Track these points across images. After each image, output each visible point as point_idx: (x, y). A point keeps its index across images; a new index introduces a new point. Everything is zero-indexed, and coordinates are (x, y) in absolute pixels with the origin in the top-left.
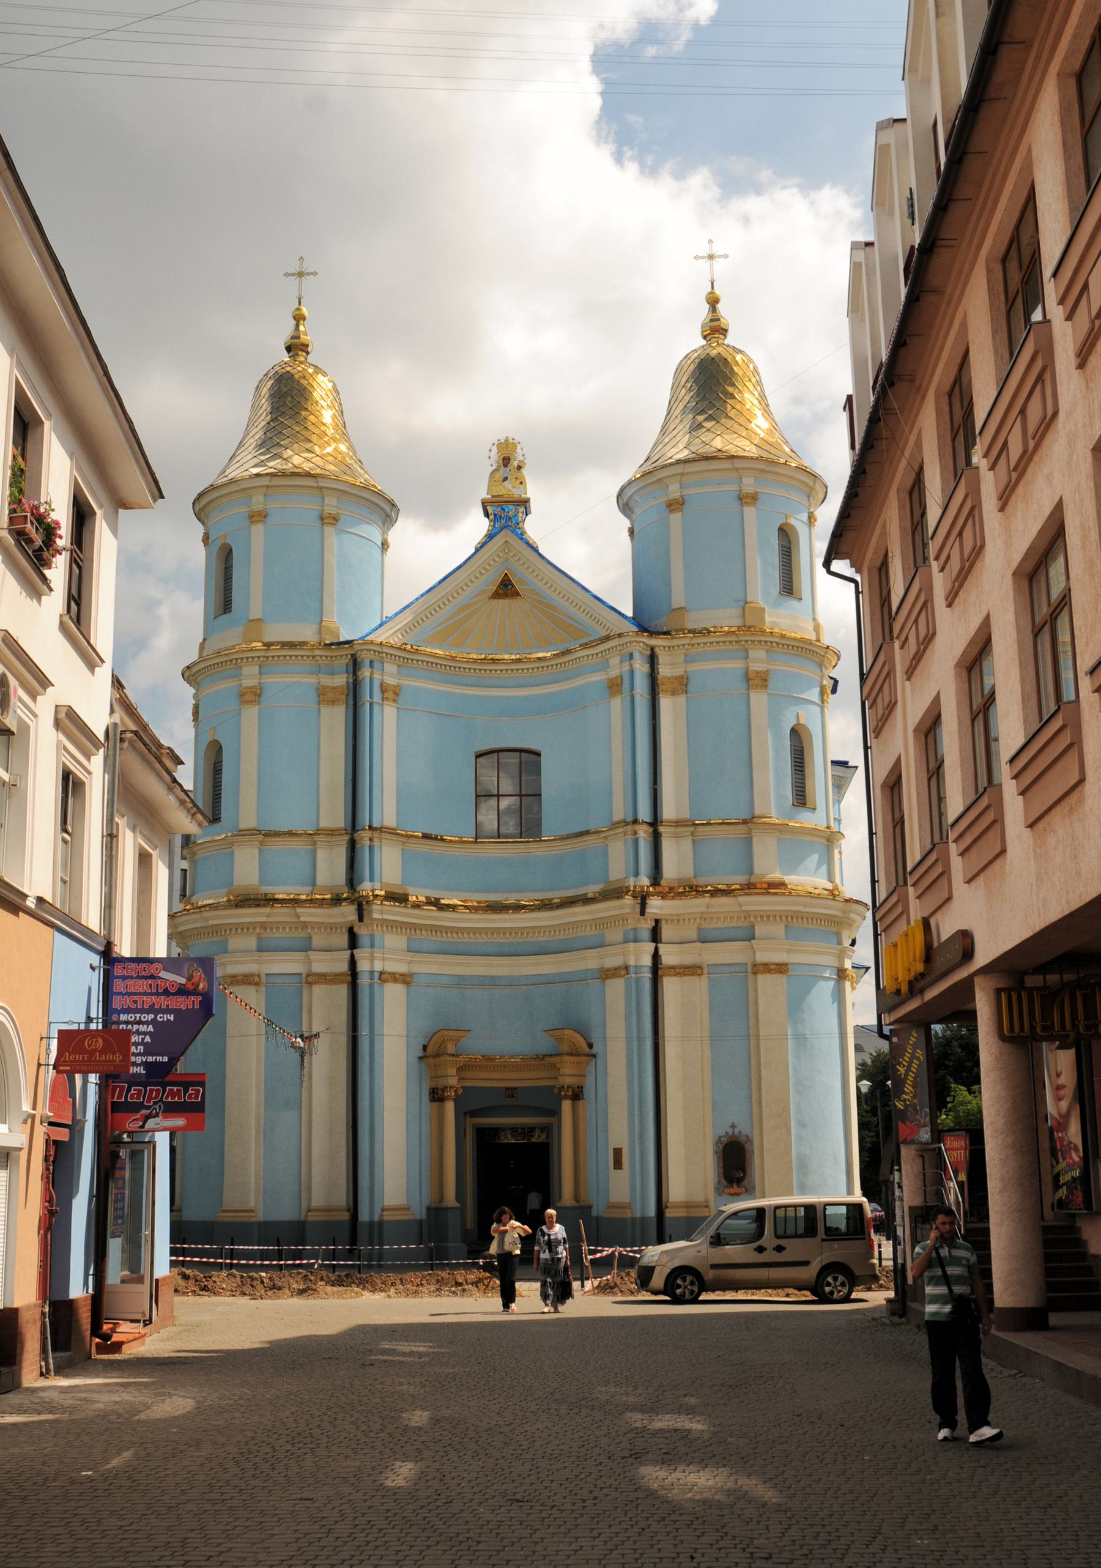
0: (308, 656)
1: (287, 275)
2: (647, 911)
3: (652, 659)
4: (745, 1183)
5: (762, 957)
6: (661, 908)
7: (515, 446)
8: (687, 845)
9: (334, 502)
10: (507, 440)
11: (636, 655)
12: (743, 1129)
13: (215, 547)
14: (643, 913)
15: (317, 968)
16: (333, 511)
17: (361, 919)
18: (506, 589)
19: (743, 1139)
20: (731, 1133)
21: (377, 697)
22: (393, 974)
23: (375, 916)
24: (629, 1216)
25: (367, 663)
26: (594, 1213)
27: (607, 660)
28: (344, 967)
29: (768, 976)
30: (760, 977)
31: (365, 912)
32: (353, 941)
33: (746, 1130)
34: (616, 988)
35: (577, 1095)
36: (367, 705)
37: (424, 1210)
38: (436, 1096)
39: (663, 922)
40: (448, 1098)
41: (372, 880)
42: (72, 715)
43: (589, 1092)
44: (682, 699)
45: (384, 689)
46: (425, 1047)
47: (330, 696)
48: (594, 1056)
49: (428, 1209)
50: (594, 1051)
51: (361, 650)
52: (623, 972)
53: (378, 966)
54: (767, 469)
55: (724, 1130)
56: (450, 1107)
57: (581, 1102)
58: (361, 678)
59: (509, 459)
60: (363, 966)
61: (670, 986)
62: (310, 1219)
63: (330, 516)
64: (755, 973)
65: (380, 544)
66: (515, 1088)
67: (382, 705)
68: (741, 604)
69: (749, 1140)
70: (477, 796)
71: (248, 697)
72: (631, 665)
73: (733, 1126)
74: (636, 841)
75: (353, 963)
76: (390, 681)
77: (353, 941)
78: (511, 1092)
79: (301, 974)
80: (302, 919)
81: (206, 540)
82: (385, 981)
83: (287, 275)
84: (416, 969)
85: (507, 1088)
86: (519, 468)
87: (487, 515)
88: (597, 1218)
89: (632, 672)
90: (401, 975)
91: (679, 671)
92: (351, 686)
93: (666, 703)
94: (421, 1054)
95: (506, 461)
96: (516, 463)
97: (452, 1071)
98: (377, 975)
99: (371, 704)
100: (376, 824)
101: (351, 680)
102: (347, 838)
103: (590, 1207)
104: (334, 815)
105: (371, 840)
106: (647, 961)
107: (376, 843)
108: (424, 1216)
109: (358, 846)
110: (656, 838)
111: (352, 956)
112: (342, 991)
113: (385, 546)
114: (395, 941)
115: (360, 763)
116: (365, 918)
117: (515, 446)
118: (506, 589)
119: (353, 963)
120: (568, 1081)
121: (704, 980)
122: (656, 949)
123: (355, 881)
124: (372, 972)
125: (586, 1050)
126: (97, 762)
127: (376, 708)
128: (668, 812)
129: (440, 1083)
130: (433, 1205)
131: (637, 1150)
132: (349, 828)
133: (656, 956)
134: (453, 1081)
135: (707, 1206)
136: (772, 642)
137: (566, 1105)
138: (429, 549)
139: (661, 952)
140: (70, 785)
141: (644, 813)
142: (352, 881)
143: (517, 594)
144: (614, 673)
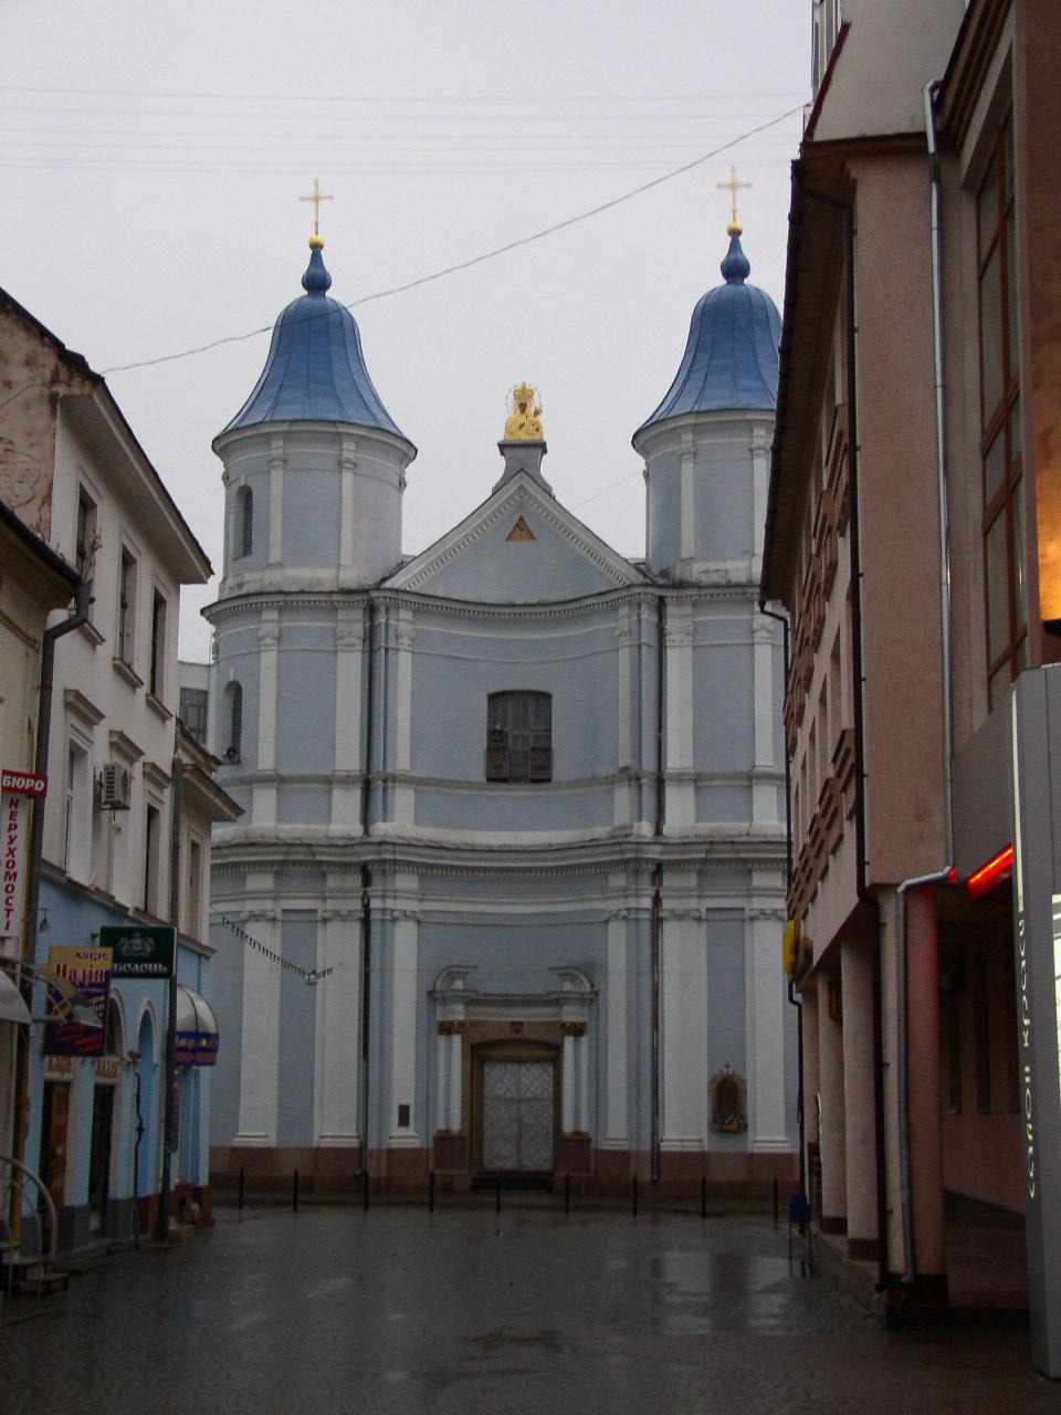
1: (302, 199)
6: (662, 853)
8: (690, 790)
9: (353, 447)
13: (235, 488)
15: (331, 905)
16: (350, 456)
19: (735, 1080)
22: (405, 911)
25: (383, 609)
26: (593, 1145)
27: (616, 609)
28: (357, 905)
32: (367, 881)
37: (431, 1141)
40: (456, 1032)
41: (385, 820)
42: (154, 766)
49: (435, 1139)
52: (625, 913)
53: (390, 904)
56: (457, 1040)
58: (376, 623)
60: (375, 904)
61: (670, 930)
63: (348, 461)
64: (752, 919)
65: (397, 483)
66: (521, 1023)
67: (398, 650)
69: (743, 1082)
71: (268, 641)
72: (639, 615)
73: (727, 1066)
74: (640, 787)
76: (404, 628)
77: (367, 881)
78: (517, 1026)
79: (315, 911)
80: (318, 858)
81: (226, 478)
82: (394, 920)
83: (302, 199)
84: (428, 906)
85: (513, 1023)
86: (537, 413)
87: (502, 454)
88: (597, 1151)
89: (639, 621)
90: (412, 912)
92: (368, 631)
94: (430, 988)
98: (388, 913)
99: (387, 649)
100: (389, 770)
102: (362, 780)
103: (589, 1140)
104: (349, 760)
105: (385, 781)
106: (647, 903)
107: (390, 784)
108: (431, 1144)
109: (372, 786)
110: (660, 784)
112: (354, 931)
113: (402, 484)
114: (406, 882)
115: (375, 705)
118: (521, 530)
122: (658, 893)
123: (369, 820)
124: (384, 910)
126: (167, 795)
127: (390, 651)
129: (450, 1018)
132: (364, 771)
133: (657, 900)
134: (461, 1017)
137: (569, 1041)
138: (441, 496)
139: (662, 894)
140: (152, 813)
141: (649, 765)
142: (366, 821)
143: (532, 537)
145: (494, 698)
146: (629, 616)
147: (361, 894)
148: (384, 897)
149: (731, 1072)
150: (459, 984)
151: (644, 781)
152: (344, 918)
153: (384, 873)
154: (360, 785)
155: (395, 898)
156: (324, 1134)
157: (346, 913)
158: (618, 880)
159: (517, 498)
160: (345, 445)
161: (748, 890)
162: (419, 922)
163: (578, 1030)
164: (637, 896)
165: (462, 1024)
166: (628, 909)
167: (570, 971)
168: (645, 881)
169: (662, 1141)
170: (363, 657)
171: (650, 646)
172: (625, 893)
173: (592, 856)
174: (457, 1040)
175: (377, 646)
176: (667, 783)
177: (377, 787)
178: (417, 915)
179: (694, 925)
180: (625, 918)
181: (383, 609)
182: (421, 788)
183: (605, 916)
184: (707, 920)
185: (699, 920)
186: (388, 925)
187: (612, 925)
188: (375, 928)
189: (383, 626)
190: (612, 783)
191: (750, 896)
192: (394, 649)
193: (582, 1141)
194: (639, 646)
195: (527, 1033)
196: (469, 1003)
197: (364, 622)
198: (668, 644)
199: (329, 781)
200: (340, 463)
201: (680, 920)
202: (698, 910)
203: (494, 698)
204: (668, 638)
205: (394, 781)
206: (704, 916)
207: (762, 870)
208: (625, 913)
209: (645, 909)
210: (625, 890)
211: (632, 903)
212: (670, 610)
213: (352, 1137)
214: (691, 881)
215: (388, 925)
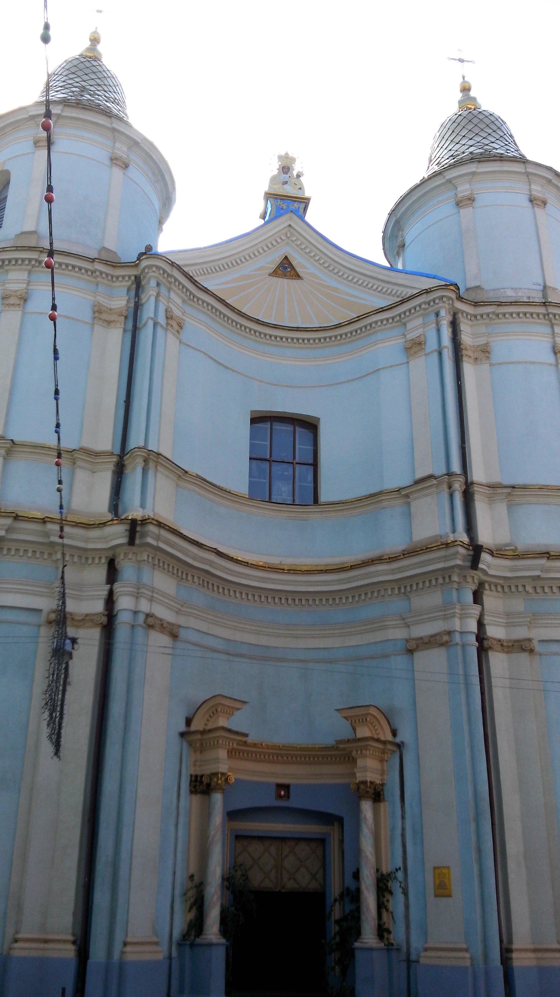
3: (454, 325)
7: (293, 160)
8: (501, 508)
9: (125, 149)
10: (287, 154)
11: (443, 313)
17: (131, 542)
18: (286, 269)
21: (162, 319)
23: (150, 540)
25: (153, 283)
27: (405, 324)
28: (99, 607)
31: (138, 535)
34: (432, 661)
35: (377, 795)
36: (151, 323)
38: (202, 786)
39: (487, 586)
40: (218, 788)
44: (485, 367)
45: (169, 317)
46: (188, 722)
47: (104, 316)
50: (398, 740)
51: (149, 267)
53: (144, 606)
57: (382, 805)
59: (289, 168)
60: (124, 603)
68: (541, 288)
70: (250, 459)
71: (12, 300)
74: (451, 496)
75: (110, 601)
79: (40, 611)
85: (280, 786)
86: (298, 176)
91: (482, 341)
95: (286, 169)
96: (295, 173)
97: (222, 754)
98: (141, 618)
100: (152, 446)
101: (132, 305)
102: (115, 459)
105: (146, 461)
107: (151, 465)
111: (111, 593)
114: (163, 582)
116: (137, 542)
117: (293, 160)
118: (286, 269)
119: (110, 601)
124: (136, 613)
125: (390, 737)
128: (478, 474)
129: (207, 770)
133: (481, 624)
134: (223, 768)
137: (367, 807)
143: (298, 276)
144: (410, 336)
145: (257, 419)
146: (424, 325)
147: (106, 593)
148: (137, 596)
154: (111, 467)
155: (151, 600)
156: (20, 936)
157: (81, 618)
158: (430, 599)
159: (283, 238)
160: (118, 145)
167: (372, 711)
170: (123, 337)
173: (393, 572)
175: (143, 322)
176: (477, 497)
177: (134, 469)
182: (181, 483)
183: (412, 645)
186: (140, 632)
188: (122, 634)
189: (153, 299)
192: (162, 326)
194: (440, 354)
195: (294, 802)
196: (232, 753)
197: (128, 302)
198: (464, 359)
200: (112, 160)
204: (464, 352)
205: (157, 463)
209: (471, 632)
212: (465, 328)
213: (65, 941)
215: (140, 632)
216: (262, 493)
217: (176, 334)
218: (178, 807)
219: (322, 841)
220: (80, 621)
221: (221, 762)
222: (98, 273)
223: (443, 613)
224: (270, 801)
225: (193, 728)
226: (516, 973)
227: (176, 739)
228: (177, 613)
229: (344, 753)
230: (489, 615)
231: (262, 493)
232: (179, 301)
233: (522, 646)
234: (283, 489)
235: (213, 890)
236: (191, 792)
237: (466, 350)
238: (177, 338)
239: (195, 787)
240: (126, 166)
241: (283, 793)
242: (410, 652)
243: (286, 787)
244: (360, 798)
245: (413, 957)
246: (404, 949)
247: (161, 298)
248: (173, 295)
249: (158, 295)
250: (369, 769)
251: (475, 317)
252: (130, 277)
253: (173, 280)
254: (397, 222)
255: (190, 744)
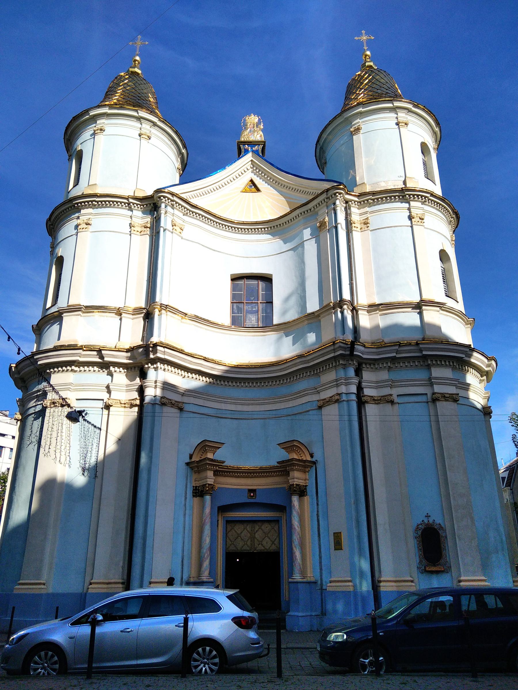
0: (125, 203)
2: (355, 353)
4: (442, 561)
5: (437, 389)
11: (338, 202)
12: (437, 518)
14: (352, 354)
19: (436, 527)
20: (426, 521)
21: (169, 227)
22: (170, 400)
23: (159, 355)
24: (351, 589)
29: (445, 403)
30: (438, 404)
32: (143, 375)
33: (439, 520)
38: (199, 492)
40: (207, 493)
43: (311, 490)
46: (191, 456)
48: (314, 463)
50: (314, 460)
51: (160, 197)
54: (414, 109)
55: (419, 518)
61: (371, 410)
62: (90, 591)
64: (434, 400)
73: (428, 516)
76: (178, 221)
85: (250, 491)
91: (364, 217)
93: (356, 235)
94: (188, 460)
97: (210, 474)
99: (164, 230)
106: (353, 389)
107: (163, 311)
116: (152, 356)
120: (296, 482)
121: (396, 406)
122: (360, 383)
130: (192, 580)
131: (355, 533)
133: (360, 388)
134: (210, 481)
135: (412, 581)
136: (425, 197)
137: (295, 500)
147: (137, 387)
149: (431, 521)
150: (210, 456)
151: (345, 307)
152: (123, 405)
153: (156, 369)
158: (330, 376)
159: (249, 168)
161: (430, 379)
162: (181, 409)
163: (302, 492)
164: (347, 384)
165: (212, 487)
166: (339, 394)
168: (351, 372)
169: (380, 582)
171: (342, 228)
172: (337, 383)
174: (208, 498)
176: (360, 312)
178: (180, 405)
179: (390, 404)
180: (337, 401)
181: (163, 205)
184: (398, 403)
185: (392, 402)
187: (326, 410)
190: (319, 316)
191: (431, 385)
192: (169, 231)
193: (309, 583)
194: (336, 228)
195: (258, 499)
196: (216, 473)
198: (353, 228)
199: (119, 312)
201: (377, 404)
202: (391, 395)
203: (235, 278)
206: (396, 400)
207: (438, 365)
208: (337, 397)
210: (336, 380)
211: (343, 389)
212: (354, 210)
214: (384, 375)
216: (237, 322)
217: (179, 234)
218: (185, 505)
219: (277, 521)
220: (125, 404)
221: (210, 477)
222: (131, 204)
223: (335, 383)
224: (244, 499)
225: (193, 460)
226: (382, 595)
227: (184, 467)
228: (182, 395)
229: (284, 468)
230: (364, 382)
231: (237, 322)
232: (181, 215)
233: (388, 400)
234: (253, 319)
235: (205, 551)
236: (194, 496)
237: (354, 223)
238: (180, 236)
239: (196, 493)
240: (149, 138)
241: (252, 494)
242: (320, 408)
243: (253, 491)
244: (292, 494)
245: (324, 587)
246: (319, 582)
247: (168, 214)
248: (176, 212)
249: (166, 212)
250: (297, 477)
251: (360, 202)
252: (150, 204)
253: (174, 203)
254: (321, 148)
255: (192, 468)
